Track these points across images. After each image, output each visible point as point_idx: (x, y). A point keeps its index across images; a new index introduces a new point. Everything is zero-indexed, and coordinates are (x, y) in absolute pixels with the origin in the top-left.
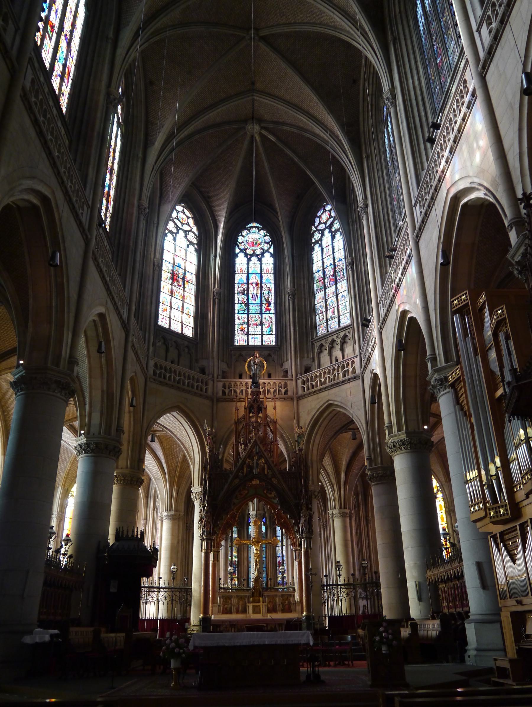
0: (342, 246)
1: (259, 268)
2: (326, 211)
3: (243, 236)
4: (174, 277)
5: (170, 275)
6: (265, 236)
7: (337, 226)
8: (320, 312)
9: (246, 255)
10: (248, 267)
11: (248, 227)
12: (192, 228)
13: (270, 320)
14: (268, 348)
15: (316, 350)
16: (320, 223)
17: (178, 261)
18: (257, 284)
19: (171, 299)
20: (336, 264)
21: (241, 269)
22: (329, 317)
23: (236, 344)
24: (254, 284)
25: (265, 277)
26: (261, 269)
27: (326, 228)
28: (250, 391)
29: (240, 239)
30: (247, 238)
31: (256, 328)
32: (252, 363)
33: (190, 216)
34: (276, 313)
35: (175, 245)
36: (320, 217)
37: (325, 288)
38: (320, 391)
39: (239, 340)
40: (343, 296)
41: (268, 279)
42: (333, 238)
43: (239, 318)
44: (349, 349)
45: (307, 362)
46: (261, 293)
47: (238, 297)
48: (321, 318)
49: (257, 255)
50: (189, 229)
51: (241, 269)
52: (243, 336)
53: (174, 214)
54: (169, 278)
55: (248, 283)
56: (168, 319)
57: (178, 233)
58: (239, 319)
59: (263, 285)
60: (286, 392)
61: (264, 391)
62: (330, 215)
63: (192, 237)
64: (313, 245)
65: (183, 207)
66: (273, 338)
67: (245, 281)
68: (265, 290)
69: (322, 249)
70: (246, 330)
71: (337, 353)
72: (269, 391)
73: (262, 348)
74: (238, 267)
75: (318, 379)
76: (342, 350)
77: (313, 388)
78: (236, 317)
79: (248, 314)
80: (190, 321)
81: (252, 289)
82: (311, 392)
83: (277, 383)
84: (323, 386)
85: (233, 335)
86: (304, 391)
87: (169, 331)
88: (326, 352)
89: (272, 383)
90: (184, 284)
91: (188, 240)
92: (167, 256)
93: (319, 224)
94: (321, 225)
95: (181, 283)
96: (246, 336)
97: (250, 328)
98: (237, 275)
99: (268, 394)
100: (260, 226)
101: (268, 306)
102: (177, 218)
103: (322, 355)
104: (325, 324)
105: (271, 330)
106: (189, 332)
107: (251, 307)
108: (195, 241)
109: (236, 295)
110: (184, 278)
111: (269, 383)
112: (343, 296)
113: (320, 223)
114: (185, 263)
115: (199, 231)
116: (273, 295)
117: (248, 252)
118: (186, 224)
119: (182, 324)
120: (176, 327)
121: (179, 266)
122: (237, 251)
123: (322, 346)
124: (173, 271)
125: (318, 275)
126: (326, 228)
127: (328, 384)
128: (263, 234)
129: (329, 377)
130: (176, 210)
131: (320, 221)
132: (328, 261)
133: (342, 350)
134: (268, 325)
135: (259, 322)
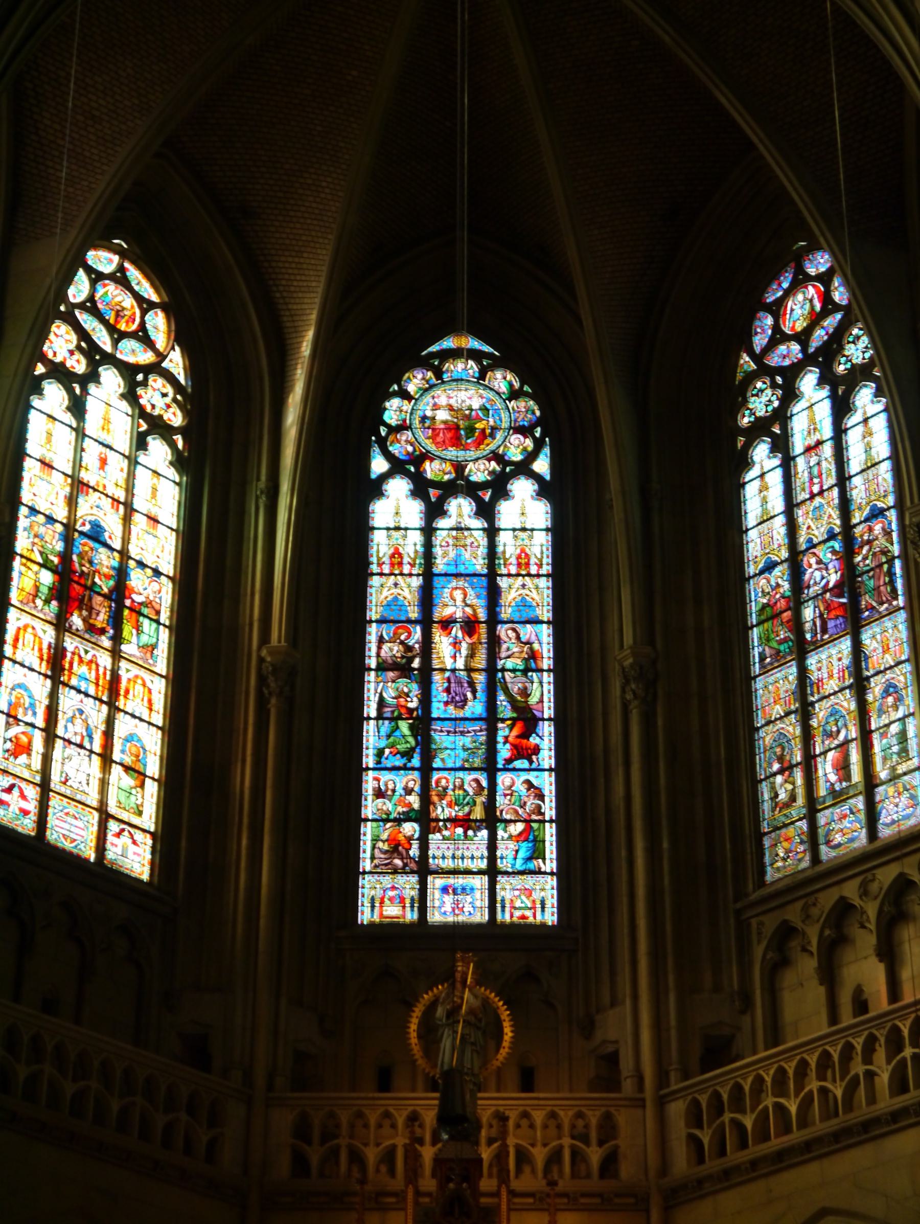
0: (882, 447)
1: (483, 551)
2: (808, 278)
3: (405, 395)
4: (68, 588)
5: (47, 578)
6: (514, 395)
7: (858, 350)
8: (776, 766)
9: (420, 487)
10: (428, 545)
11: (433, 355)
12: (162, 357)
13: (531, 802)
14: (524, 936)
15: (759, 951)
16: (778, 337)
18: (470, 626)
19: (53, 696)
20: (858, 531)
21: (397, 554)
22: (822, 791)
23: (365, 916)
24: (457, 631)
25: (512, 591)
26: (492, 554)
27: (808, 360)
28: (428, 1153)
30: (425, 407)
32: (440, 1012)
33: (155, 298)
34: (561, 770)
35: (80, 433)
36: (777, 309)
37: (801, 649)
38: (782, 1160)
39: (381, 898)
40: (890, 689)
41: (524, 604)
42: (842, 408)
46: (491, 670)
48: (783, 796)
49: (472, 490)
50: (146, 357)
51: (397, 554)
52: (401, 880)
53: (79, 289)
54: (44, 590)
55: (426, 621)
56: (32, 793)
57: (92, 376)
58: (379, 794)
59: (503, 631)
60: (609, 1165)
61: (501, 1157)
62: (826, 298)
63: (157, 396)
64: (741, 440)
65: (123, 254)
66: (547, 889)
67: (414, 614)
68: (511, 659)
69: (787, 464)
70: (414, 851)
71: (865, 970)
72: (523, 1157)
73: (494, 941)
74: (380, 544)
75: (769, 1101)
76: (889, 953)
77: (743, 1144)
78: (369, 783)
79: (426, 770)
81: (447, 651)
82: (737, 1168)
83: (566, 1117)
84: (797, 1136)
85: (353, 873)
86: (701, 1160)
88: (808, 965)
89: (538, 1117)
90: (116, 621)
91: (143, 414)
92: (41, 490)
93: (773, 343)
94: (782, 349)
95: (101, 619)
96: (414, 879)
97: (435, 838)
98: (375, 581)
99: (519, 1171)
100: (487, 349)
101: (525, 735)
102: (91, 306)
103: (789, 978)
104: (803, 825)
105: (537, 853)
106: (135, 857)
107: (441, 739)
108: (176, 418)
109: (371, 677)
110: (120, 590)
111: (525, 1115)
112: (890, 689)
113: (778, 337)
114: (127, 520)
115: (192, 368)
116: (548, 678)
117: (431, 470)
118: (133, 335)
119: (105, 816)
120: (72, 832)
121: (96, 535)
122: (379, 465)
123: (787, 932)
124: (65, 557)
126: (808, 360)
127: (820, 1127)
128: (503, 388)
129: (824, 1091)
130: (89, 270)
131: (776, 328)
132: (819, 520)
133: (889, 953)
134: (520, 827)
135: (478, 813)
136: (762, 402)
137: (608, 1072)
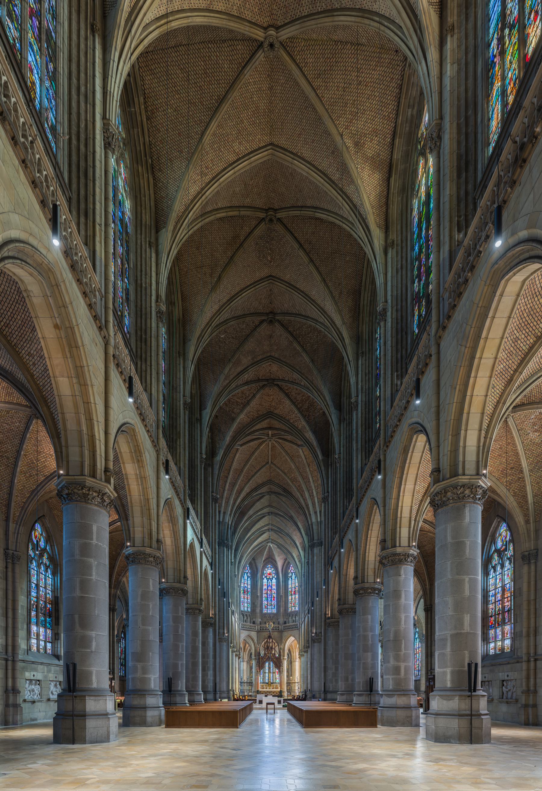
14: (273, 614)
17: (246, 585)
39: (265, 611)
44: (297, 618)
45: (285, 620)
63: (249, 574)
71: (294, 618)
125: (290, 590)
132: (293, 586)
136: (290, 575)
137: (279, 623)
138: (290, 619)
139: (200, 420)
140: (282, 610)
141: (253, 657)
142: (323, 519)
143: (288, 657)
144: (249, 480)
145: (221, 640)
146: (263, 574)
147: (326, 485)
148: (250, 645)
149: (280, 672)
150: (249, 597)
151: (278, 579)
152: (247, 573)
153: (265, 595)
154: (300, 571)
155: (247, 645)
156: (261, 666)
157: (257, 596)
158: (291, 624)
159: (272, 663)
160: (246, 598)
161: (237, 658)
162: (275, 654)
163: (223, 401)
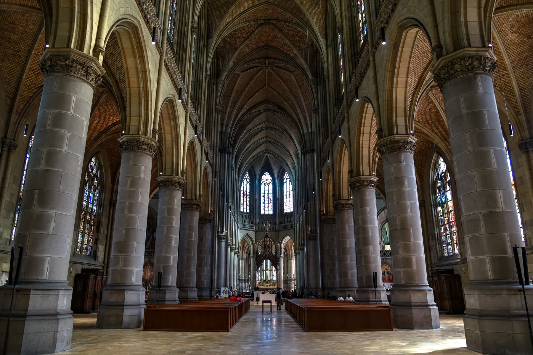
29: (262, 178)
31: (267, 209)
39: (262, 212)
43: (262, 205)
44: (292, 219)
47: (262, 198)
63: (248, 180)
71: (289, 219)
80: (248, 207)
87: (243, 212)
120: (245, 211)
125: (285, 194)
132: (288, 190)
136: (285, 180)
137: (275, 224)
138: (286, 220)
139: (207, 46)
140: (278, 211)
141: (251, 255)
142: (314, 130)
143: (284, 255)
144: (249, 99)
145: (220, 239)
146: (260, 179)
147: (316, 100)
148: (248, 244)
149: (277, 270)
150: (248, 200)
151: (274, 184)
152: (247, 179)
153: (263, 198)
154: (294, 177)
155: (246, 244)
156: (259, 264)
157: (256, 199)
158: (286, 224)
159: (269, 261)
160: (245, 200)
161: (236, 256)
162: (271, 252)
163: (226, 33)
